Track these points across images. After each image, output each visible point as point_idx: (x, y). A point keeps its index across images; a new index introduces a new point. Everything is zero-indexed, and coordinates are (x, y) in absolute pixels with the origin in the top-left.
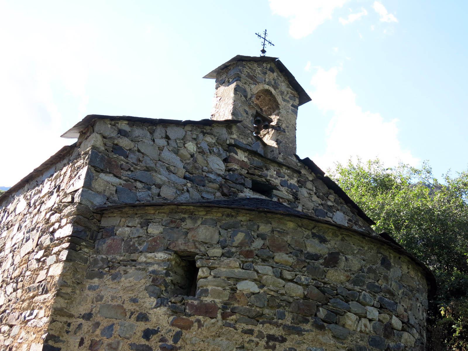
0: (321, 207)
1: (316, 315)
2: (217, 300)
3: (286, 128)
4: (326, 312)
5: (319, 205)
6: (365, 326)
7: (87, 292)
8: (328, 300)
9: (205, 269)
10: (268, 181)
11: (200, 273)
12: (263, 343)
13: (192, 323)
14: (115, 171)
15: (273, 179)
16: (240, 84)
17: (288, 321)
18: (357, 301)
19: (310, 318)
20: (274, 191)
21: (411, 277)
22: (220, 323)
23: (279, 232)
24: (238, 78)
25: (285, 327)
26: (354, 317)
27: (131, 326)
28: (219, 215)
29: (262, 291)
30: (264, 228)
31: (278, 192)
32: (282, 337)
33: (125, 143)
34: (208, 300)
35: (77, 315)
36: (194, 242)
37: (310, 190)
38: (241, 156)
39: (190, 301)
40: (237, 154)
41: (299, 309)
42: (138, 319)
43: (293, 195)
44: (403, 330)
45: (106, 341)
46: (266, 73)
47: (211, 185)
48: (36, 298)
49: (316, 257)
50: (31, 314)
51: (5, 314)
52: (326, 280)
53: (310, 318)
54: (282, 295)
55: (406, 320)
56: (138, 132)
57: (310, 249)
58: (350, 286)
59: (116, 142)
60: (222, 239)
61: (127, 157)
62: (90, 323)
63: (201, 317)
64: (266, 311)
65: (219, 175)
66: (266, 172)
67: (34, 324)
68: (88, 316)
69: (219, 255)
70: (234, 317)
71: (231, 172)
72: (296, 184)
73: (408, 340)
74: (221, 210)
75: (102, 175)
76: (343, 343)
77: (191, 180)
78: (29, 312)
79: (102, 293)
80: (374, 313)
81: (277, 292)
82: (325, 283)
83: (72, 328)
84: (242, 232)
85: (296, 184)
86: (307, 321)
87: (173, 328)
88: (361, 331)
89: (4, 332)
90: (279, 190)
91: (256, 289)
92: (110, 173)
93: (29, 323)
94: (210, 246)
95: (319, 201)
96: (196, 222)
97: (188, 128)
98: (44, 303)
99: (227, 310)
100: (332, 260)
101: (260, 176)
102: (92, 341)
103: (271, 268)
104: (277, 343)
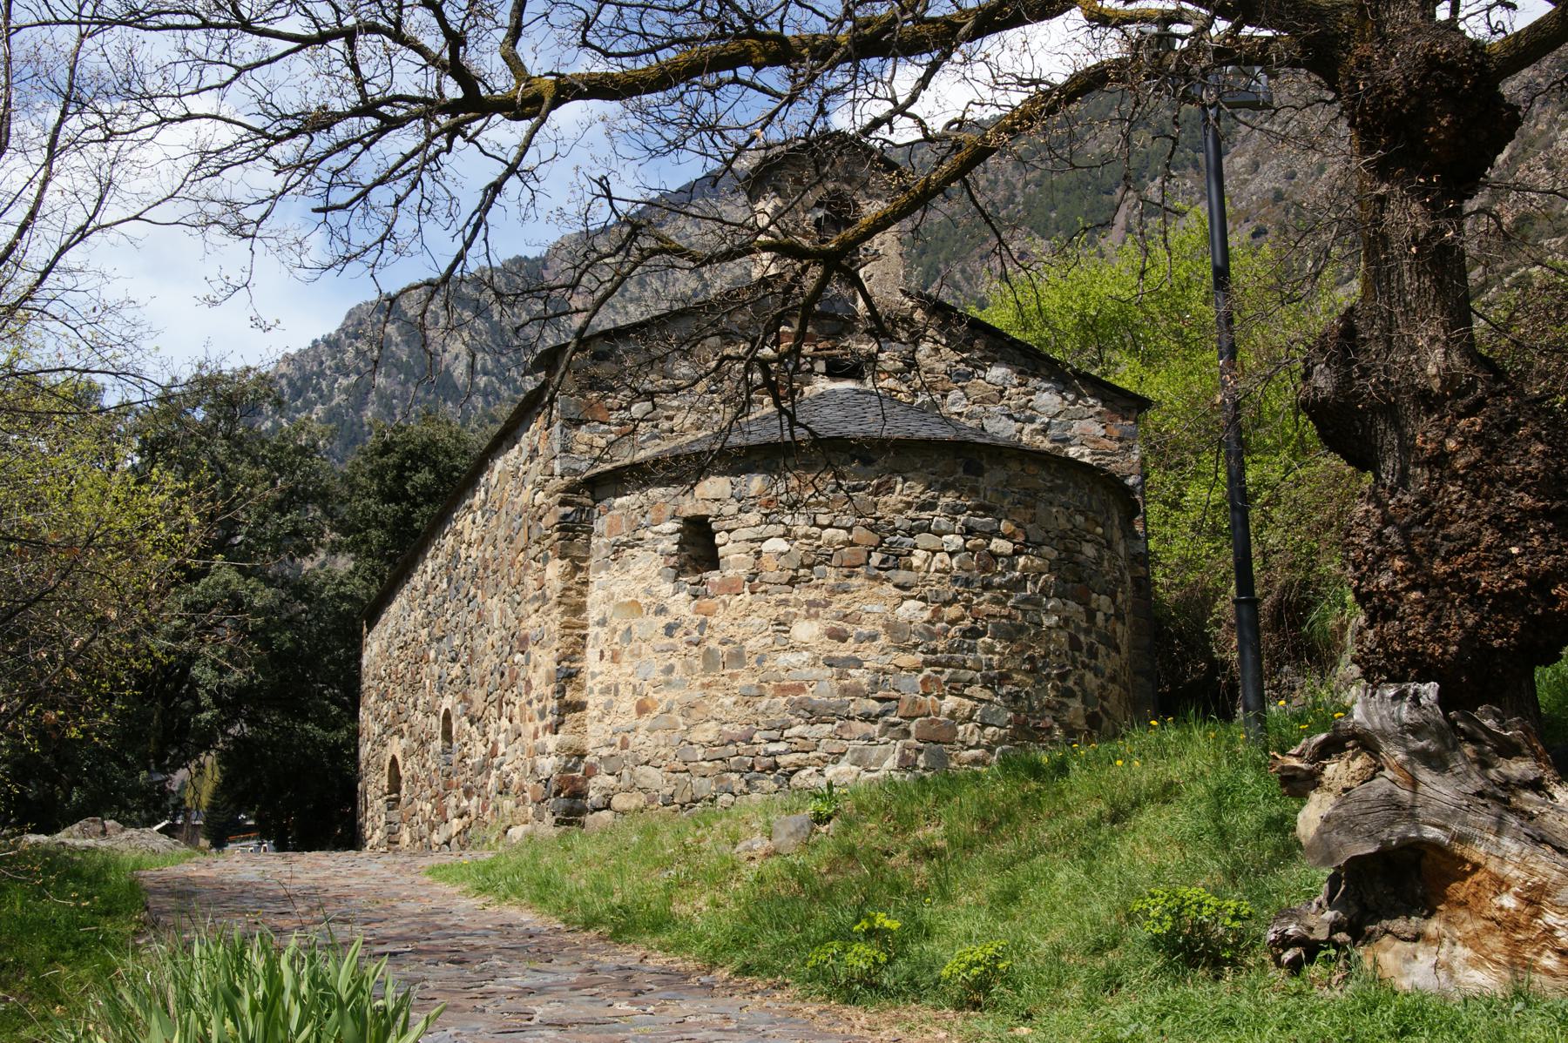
0: (961, 366)
11: (718, 540)
14: (599, 416)
34: (730, 573)
42: (657, 613)
68: (603, 623)
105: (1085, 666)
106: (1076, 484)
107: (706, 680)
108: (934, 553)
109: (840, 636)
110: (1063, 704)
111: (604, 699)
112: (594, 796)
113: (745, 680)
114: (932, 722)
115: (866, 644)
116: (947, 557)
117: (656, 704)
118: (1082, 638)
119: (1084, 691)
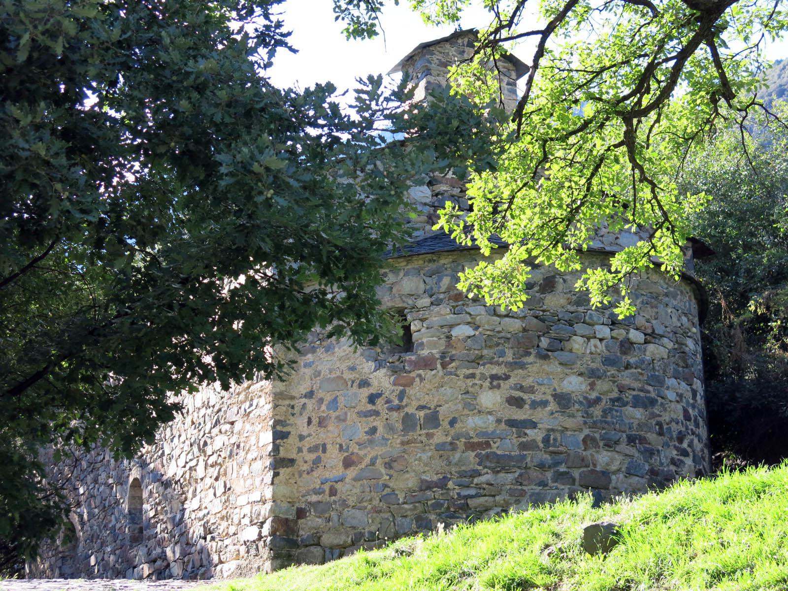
1: (538, 346)
2: (434, 351)
4: (548, 341)
6: (595, 346)
7: (303, 370)
8: (549, 328)
9: (416, 322)
12: (487, 384)
13: (414, 378)
16: (431, 79)
17: (509, 357)
19: (532, 350)
21: (652, 282)
22: (441, 373)
24: (427, 72)
25: (507, 364)
26: (580, 340)
27: (355, 395)
28: (421, 262)
29: (477, 333)
32: (505, 374)
34: (425, 352)
35: (298, 395)
36: (400, 296)
39: (407, 358)
41: (519, 343)
44: (646, 342)
45: (333, 414)
46: (464, 52)
48: (252, 387)
50: (251, 405)
51: (221, 413)
52: (545, 307)
53: (532, 350)
54: (499, 332)
55: (650, 331)
60: (428, 287)
62: (313, 401)
63: (421, 372)
64: (485, 352)
65: (425, 204)
67: (257, 414)
68: (310, 394)
69: (428, 304)
70: (453, 364)
71: (440, 197)
73: (656, 352)
74: (421, 256)
78: (248, 404)
79: (319, 368)
80: (605, 331)
81: (493, 330)
82: (544, 311)
83: (297, 410)
84: (447, 275)
86: (530, 354)
87: (396, 388)
88: (591, 353)
89: (226, 431)
91: (472, 333)
93: (251, 415)
94: (417, 297)
96: (398, 275)
98: (261, 391)
99: (445, 359)
102: (319, 418)
104: (501, 382)
105: (693, 433)
106: (682, 292)
107: (405, 439)
108: (589, 339)
110: (682, 461)
111: (313, 456)
112: (304, 533)
113: (439, 437)
114: (592, 471)
115: (539, 409)
116: (598, 342)
117: (361, 459)
118: (690, 411)
119: (693, 451)
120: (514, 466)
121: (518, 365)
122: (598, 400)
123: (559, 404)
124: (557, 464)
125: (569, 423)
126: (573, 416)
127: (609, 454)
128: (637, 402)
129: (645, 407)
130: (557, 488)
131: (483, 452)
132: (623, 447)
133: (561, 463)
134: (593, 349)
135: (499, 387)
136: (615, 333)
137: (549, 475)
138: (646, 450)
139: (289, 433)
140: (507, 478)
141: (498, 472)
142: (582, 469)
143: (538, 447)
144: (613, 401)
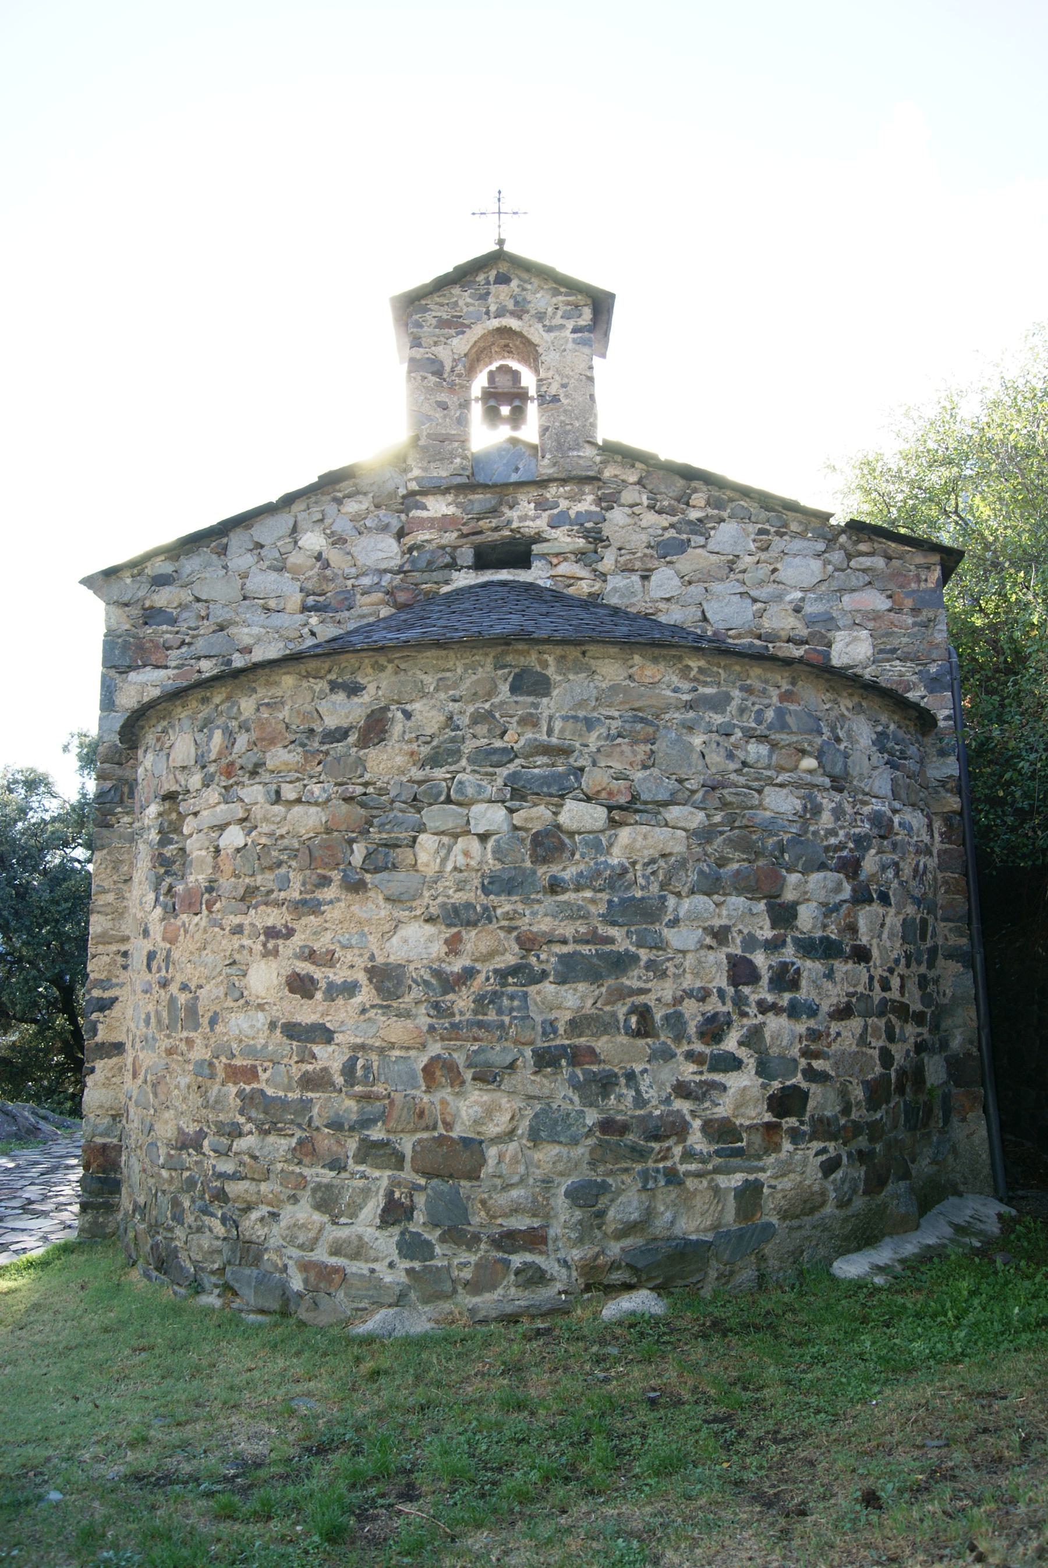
0: (671, 533)
3: (562, 393)
5: (665, 529)
6: (466, 854)
10: (517, 531)
14: (153, 659)
15: (527, 524)
18: (449, 801)
20: (534, 547)
23: (267, 705)
30: (247, 705)
31: (545, 544)
33: (164, 598)
37: (631, 506)
38: (439, 507)
40: (425, 508)
43: (585, 537)
46: (488, 294)
47: (366, 599)
49: (340, 734)
52: (367, 777)
56: (190, 565)
57: (331, 722)
58: (417, 774)
59: (147, 604)
61: (173, 621)
65: (386, 571)
66: (509, 514)
72: (594, 508)
75: (133, 676)
76: (411, 909)
77: (316, 608)
80: (491, 817)
82: (366, 785)
85: (594, 508)
86: (325, 882)
90: (548, 540)
92: (145, 666)
95: (665, 520)
97: (298, 507)
100: (375, 729)
101: (496, 529)
103: (260, 787)
104: (280, 942)
109: (301, 986)
114: (441, 1140)
115: (340, 1001)
116: (475, 845)
120: (292, 1122)
121: (308, 906)
122: (469, 974)
123: (378, 989)
124: (366, 1123)
125: (397, 1030)
126: (407, 1015)
127: (485, 1098)
128: (570, 970)
129: (594, 976)
130: (364, 1177)
131: (248, 1088)
132: (526, 1077)
133: (374, 1121)
134: (461, 861)
135: (275, 953)
136: (518, 819)
137: (352, 1145)
138: (593, 1078)
139: (114, 1000)
140: (281, 1145)
141: (267, 1132)
142: (419, 1135)
143: (333, 1084)
144: (502, 975)
